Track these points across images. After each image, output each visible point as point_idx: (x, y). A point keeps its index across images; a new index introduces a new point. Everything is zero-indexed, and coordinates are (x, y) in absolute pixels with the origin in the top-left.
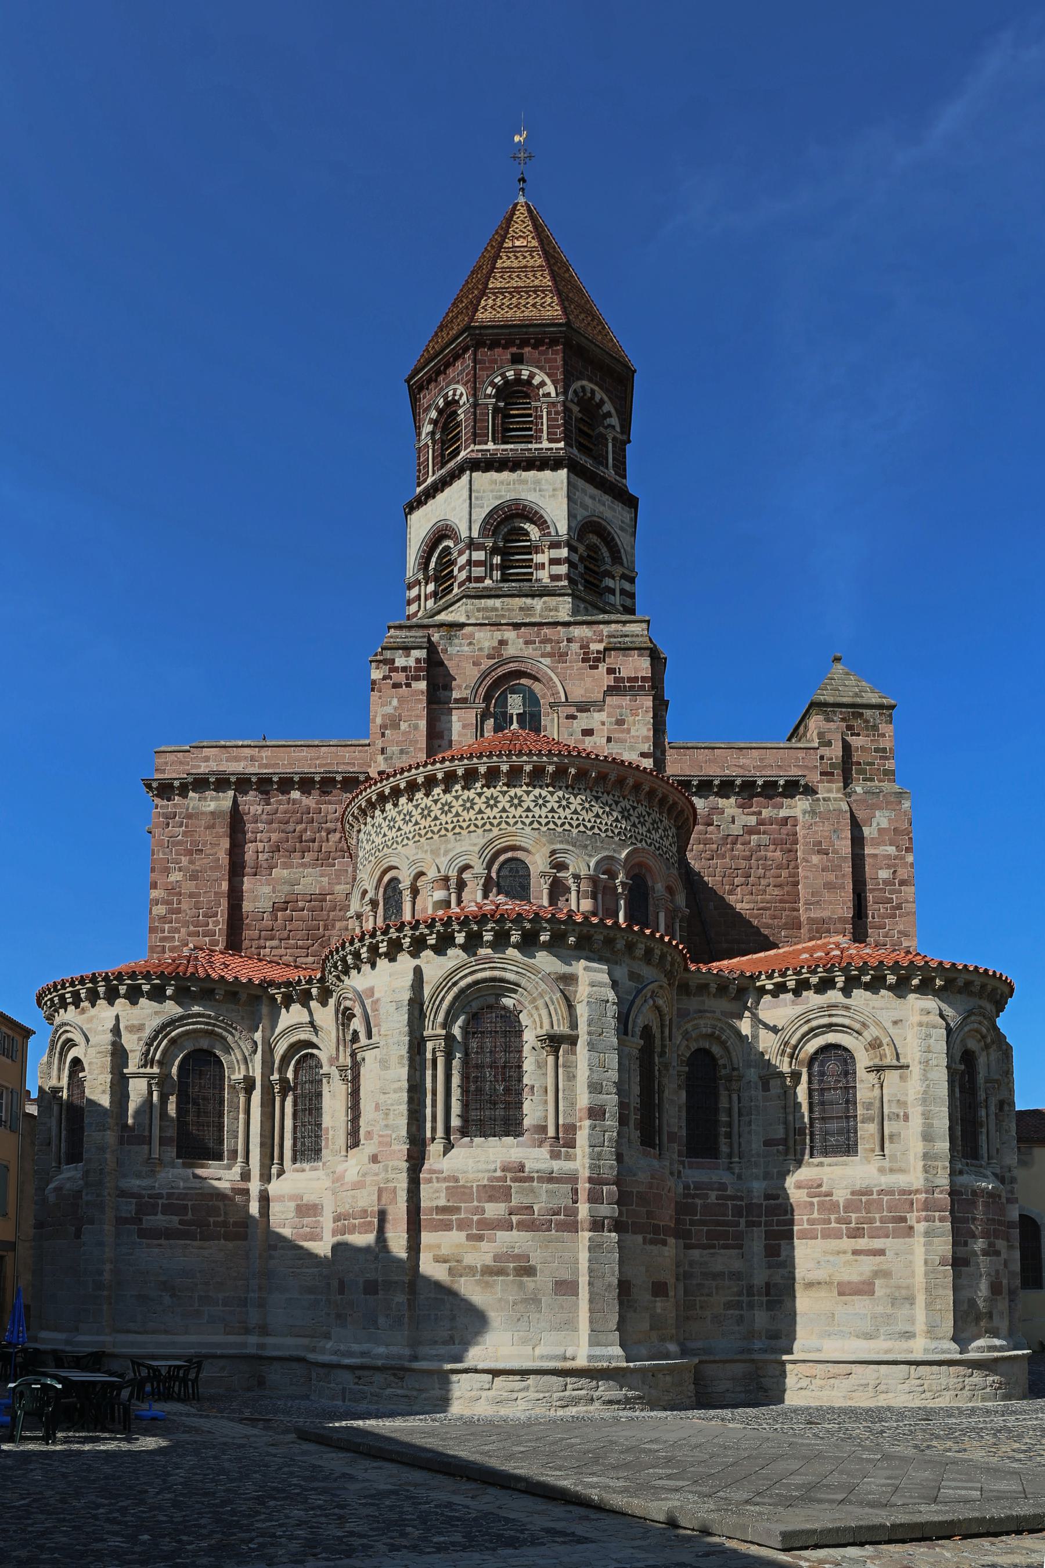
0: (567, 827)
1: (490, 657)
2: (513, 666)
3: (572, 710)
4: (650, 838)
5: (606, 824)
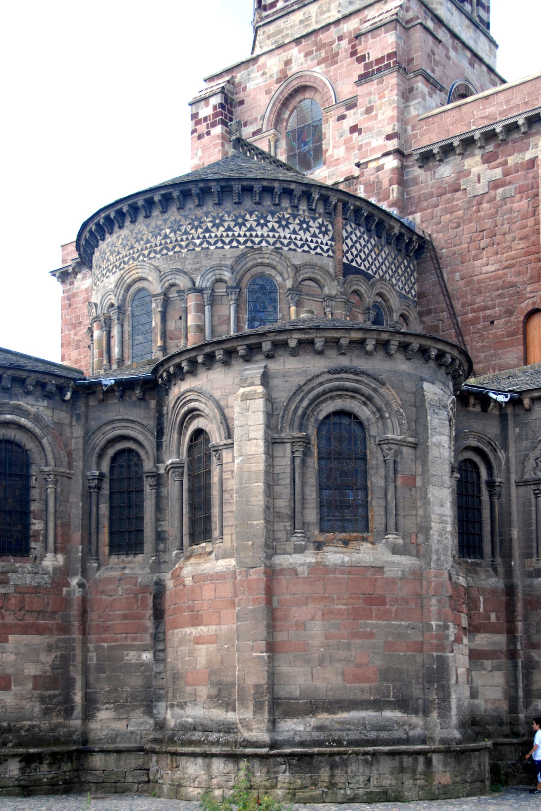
0: (177, 249)
1: (278, 81)
2: (295, 84)
3: (342, 111)
4: (274, 237)
5: (216, 236)
